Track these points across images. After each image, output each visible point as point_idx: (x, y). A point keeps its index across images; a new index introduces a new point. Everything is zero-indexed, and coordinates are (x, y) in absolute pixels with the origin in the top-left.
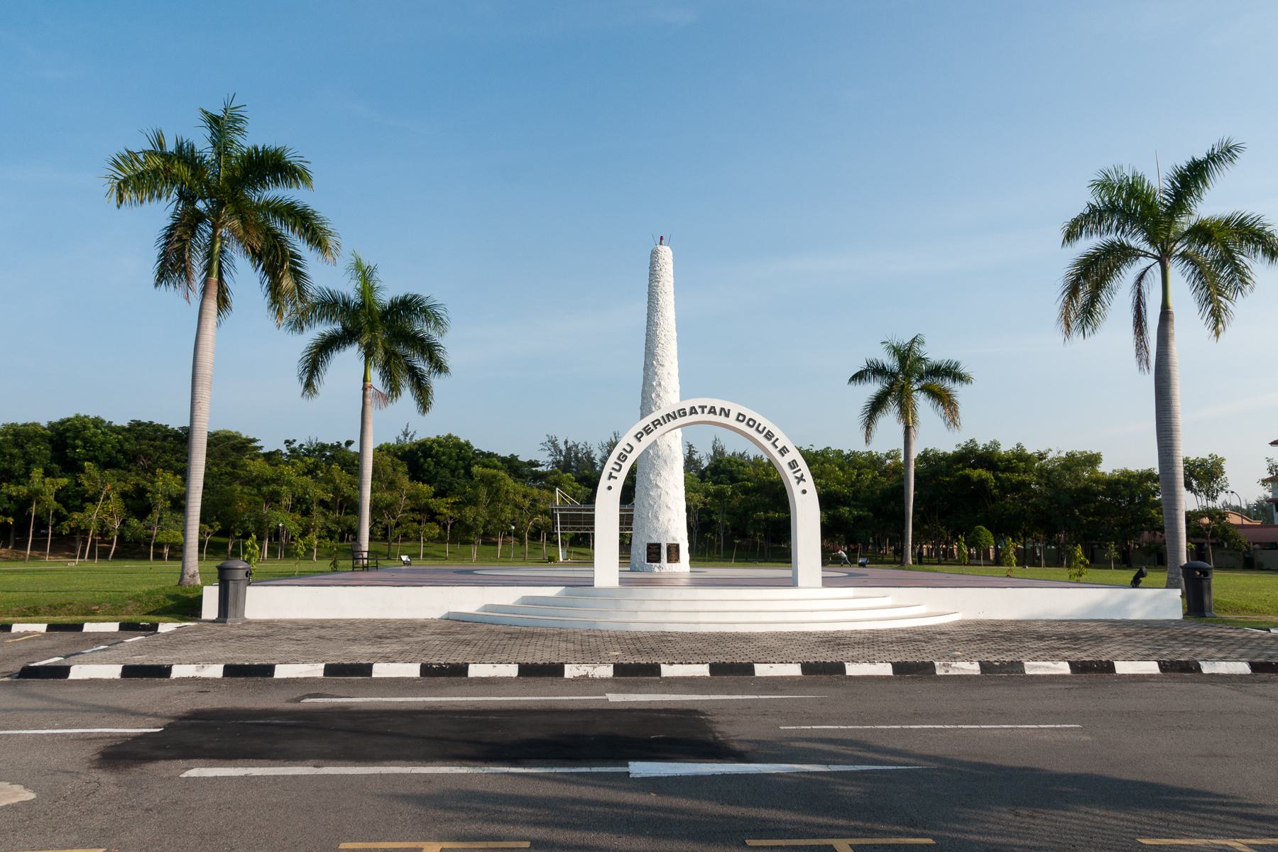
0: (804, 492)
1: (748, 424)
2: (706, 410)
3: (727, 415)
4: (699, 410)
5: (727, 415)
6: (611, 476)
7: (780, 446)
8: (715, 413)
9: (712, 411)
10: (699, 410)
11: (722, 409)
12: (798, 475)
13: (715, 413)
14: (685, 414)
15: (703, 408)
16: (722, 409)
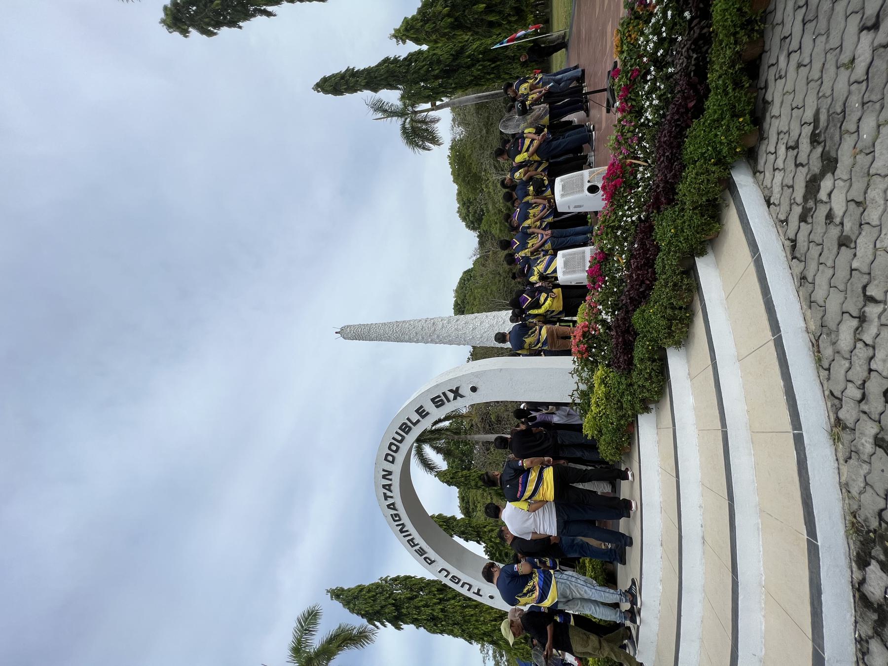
0: (474, 389)
1: (396, 452)
2: (389, 494)
3: (390, 473)
4: (390, 501)
5: (390, 473)
6: (478, 594)
7: (415, 417)
8: (390, 485)
9: (388, 487)
10: (390, 501)
11: (384, 477)
12: (451, 396)
13: (390, 485)
14: (396, 515)
15: (386, 497)
16: (384, 477)
